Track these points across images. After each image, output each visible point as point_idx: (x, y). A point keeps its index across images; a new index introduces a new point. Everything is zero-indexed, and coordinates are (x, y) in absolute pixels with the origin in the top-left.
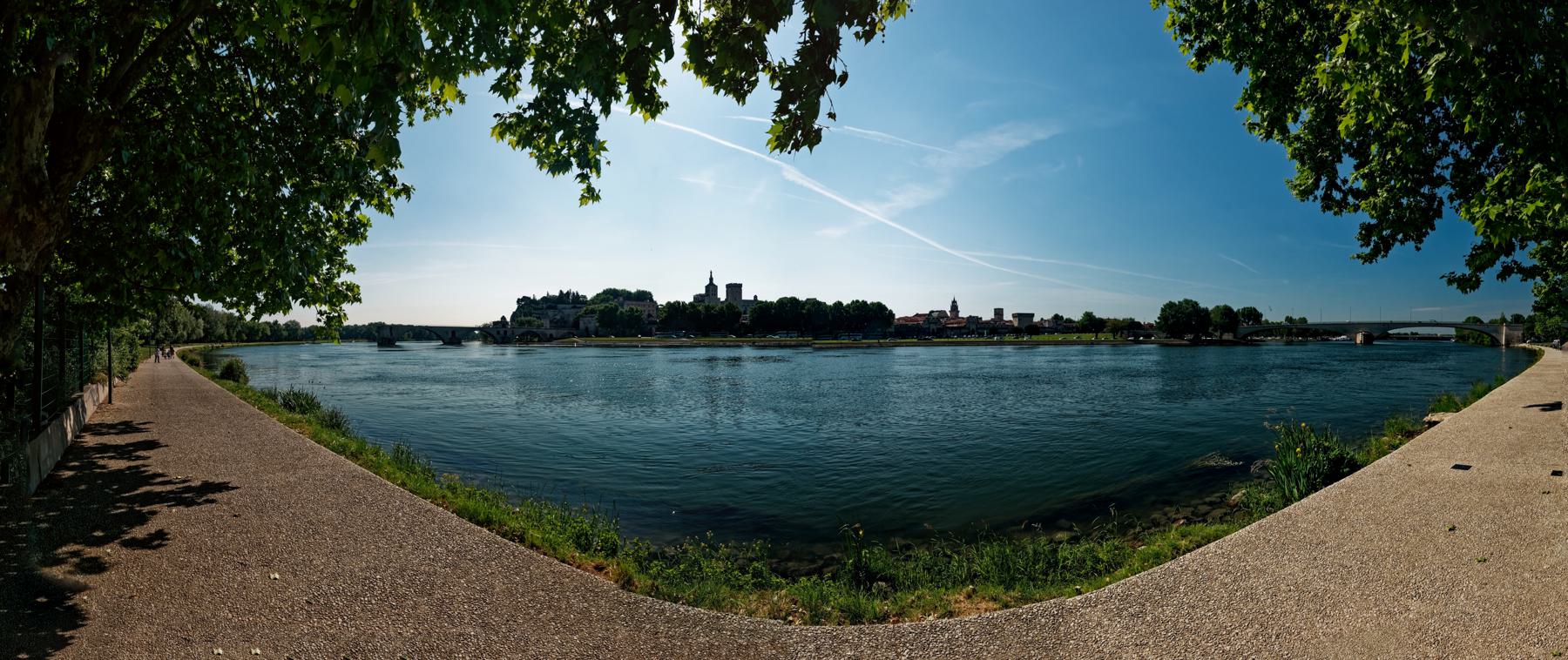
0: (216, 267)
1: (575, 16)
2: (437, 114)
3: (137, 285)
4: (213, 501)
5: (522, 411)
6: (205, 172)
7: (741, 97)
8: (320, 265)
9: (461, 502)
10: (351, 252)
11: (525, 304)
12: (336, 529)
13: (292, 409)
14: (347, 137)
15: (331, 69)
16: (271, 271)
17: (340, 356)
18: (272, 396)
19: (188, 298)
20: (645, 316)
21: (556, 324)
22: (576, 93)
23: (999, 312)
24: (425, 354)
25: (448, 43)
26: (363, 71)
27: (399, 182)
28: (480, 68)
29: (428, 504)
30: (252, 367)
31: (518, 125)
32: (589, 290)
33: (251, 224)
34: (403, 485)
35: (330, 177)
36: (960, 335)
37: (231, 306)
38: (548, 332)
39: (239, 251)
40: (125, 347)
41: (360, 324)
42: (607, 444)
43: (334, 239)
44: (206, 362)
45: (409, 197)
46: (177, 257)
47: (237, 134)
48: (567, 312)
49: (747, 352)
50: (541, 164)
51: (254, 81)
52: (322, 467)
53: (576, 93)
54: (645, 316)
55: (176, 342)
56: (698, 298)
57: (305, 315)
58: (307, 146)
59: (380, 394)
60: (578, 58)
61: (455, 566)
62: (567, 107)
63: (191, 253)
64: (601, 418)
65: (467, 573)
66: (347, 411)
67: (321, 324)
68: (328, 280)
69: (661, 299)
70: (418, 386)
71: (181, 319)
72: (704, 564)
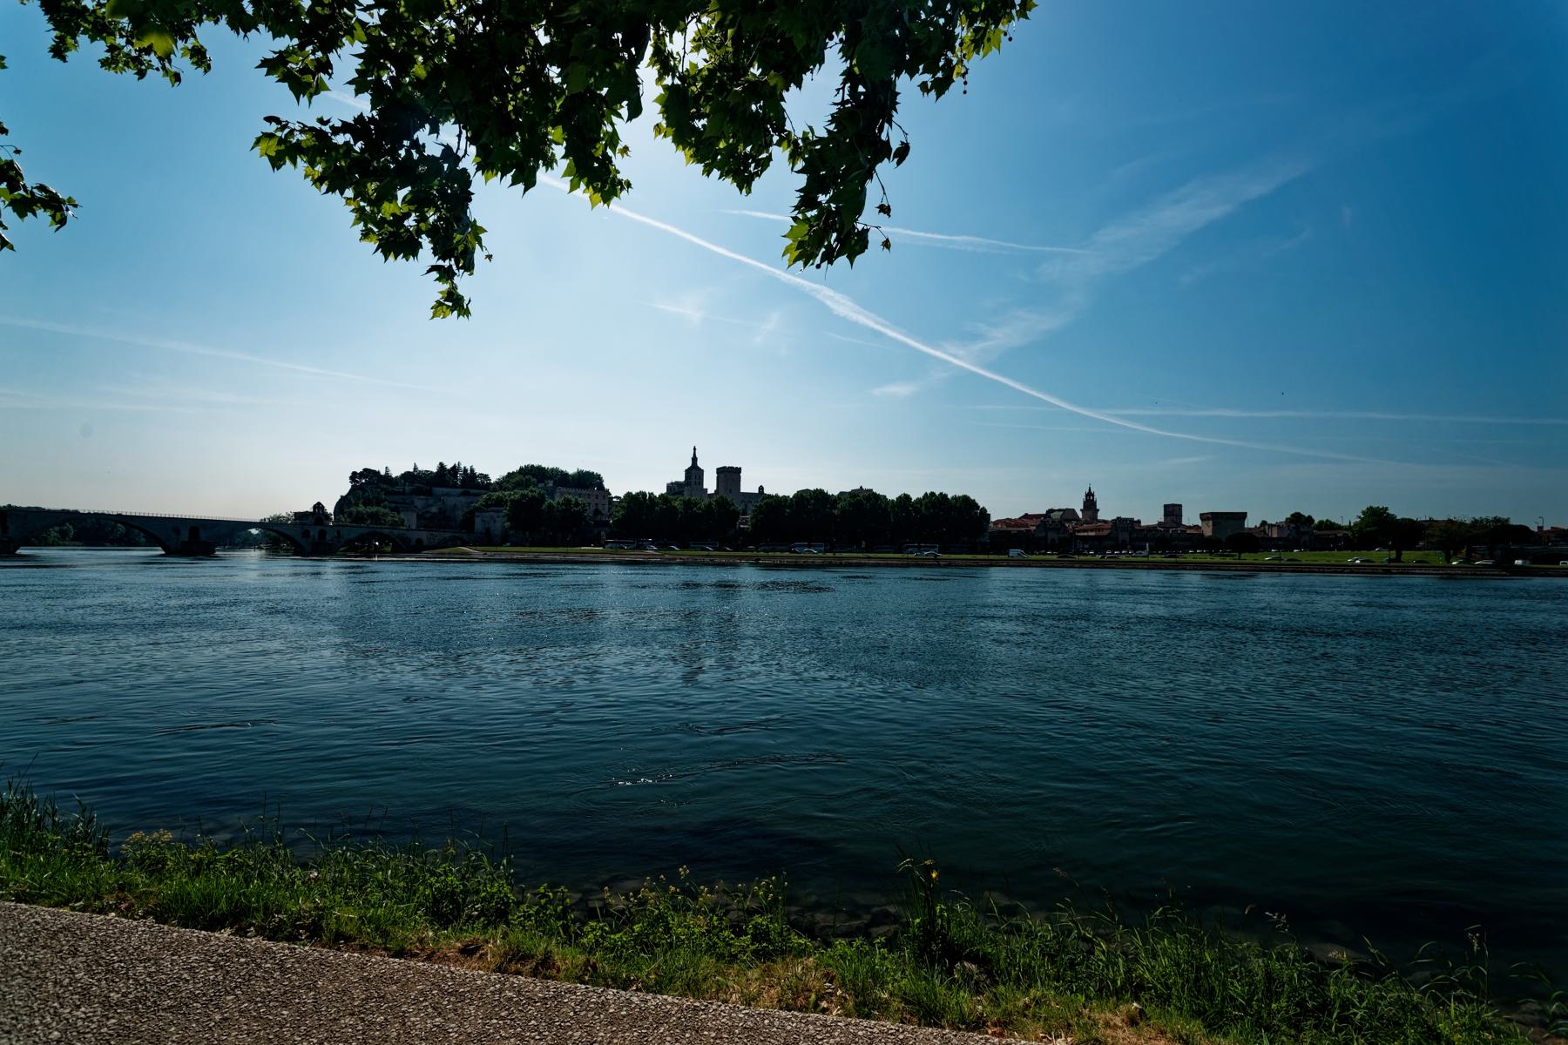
7: (745, 182)
11: (368, 484)
20: (589, 513)
21: (426, 521)
23: (1173, 511)
36: (1029, 550)
48: (451, 501)
54: (589, 513)
56: (673, 488)
69: (617, 487)
72: (673, 921)
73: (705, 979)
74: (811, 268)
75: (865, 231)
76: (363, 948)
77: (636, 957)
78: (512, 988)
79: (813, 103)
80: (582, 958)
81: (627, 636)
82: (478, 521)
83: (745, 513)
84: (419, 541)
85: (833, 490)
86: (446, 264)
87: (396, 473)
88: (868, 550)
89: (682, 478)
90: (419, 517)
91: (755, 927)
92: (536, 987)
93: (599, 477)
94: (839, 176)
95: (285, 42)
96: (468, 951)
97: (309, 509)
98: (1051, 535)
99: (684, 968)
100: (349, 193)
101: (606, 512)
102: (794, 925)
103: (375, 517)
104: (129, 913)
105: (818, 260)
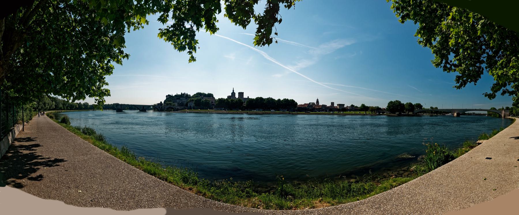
0: (59, 83)
3: (32, 90)
5: (167, 135)
6: (55, 50)
8: (96, 82)
9: (145, 167)
10: (107, 78)
11: (169, 97)
12: (101, 176)
13: (86, 134)
14: (106, 36)
15: (100, 11)
16: (78, 85)
17: (103, 115)
18: (79, 129)
19: (49, 94)
20: (210, 102)
22: (188, 22)
24: (133, 115)
25: (143, 3)
26: (112, 12)
27: (124, 53)
28: (154, 12)
29: (134, 168)
30: (72, 119)
31: (167, 33)
32: (192, 93)
33: (71, 68)
34: (125, 161)
35: (100, 51)
37: (64, 97)
38: (177, 107)
39: (67, 78)
40: (28, 112)
41: (110, 104)
42: (197, 147)
43: (101, 73)
44: (56, 117)
45: (128, 58)
46: (46, 80)
47: (67, 35)
48: (183, 100)
49: (245, 116)
50: (175, 47)
51: (73, 16)
52: (96, 154)
53: (188, 22)
54: (210, 102)
55: (45, 110)
56: (229, 97)
57: (90, 101)
58: (91, 40)
59: (117, 129)
60: (189, 10)
61: (143, 189)
62: (185, 27)
63: (51, 78)
64: (195, 138)
66: (105, 135)
67: (96, 104)
68: (99, 88)
69: (217, 97)
70: (131, 126)
71: (47, 102)
80: (210, 194)
87: (174, 95)
96: (190, 189)
103: (170, 104)
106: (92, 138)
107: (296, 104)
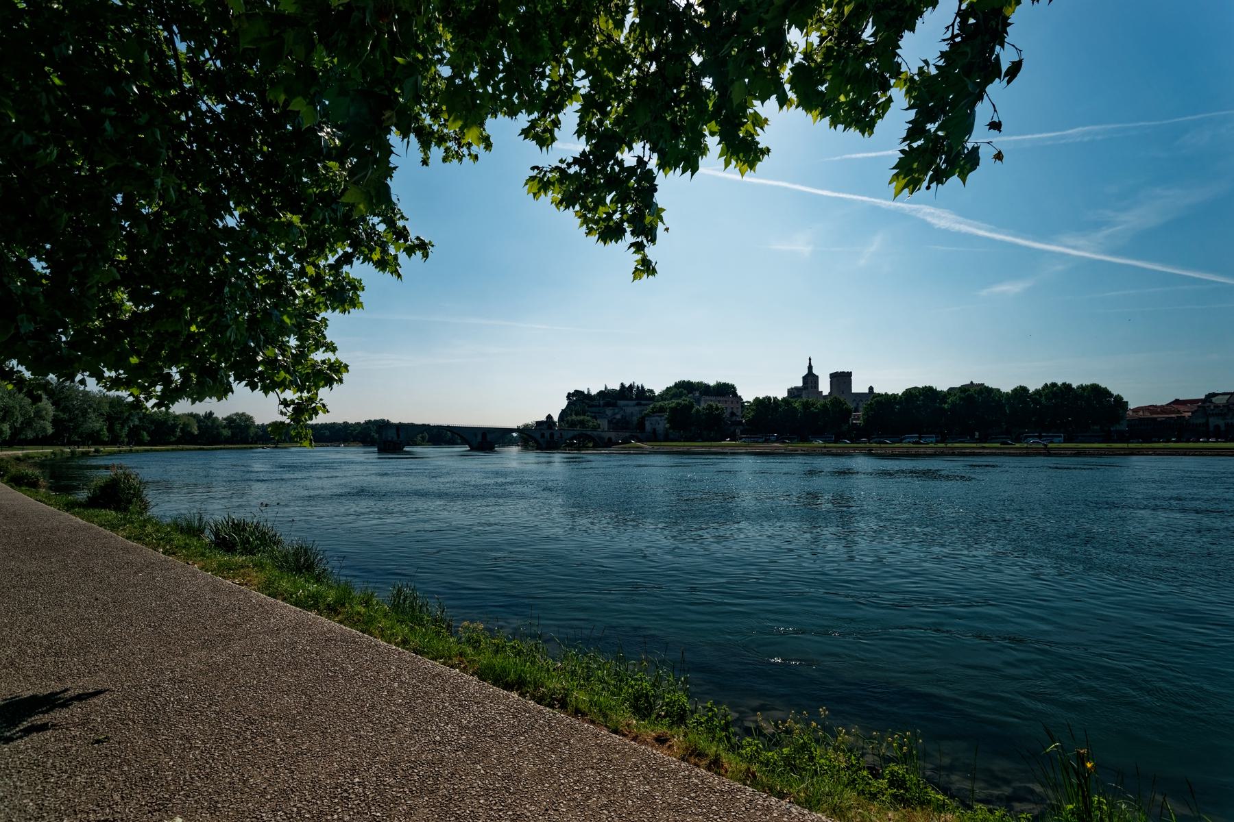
1: (629, 60)
2: (460, 158)
4: (43, 728)
9: (484, 659)
11: (577, 399)
17: (313, 466)
18: (192, 530)
20: (727, 414)
21: (616, 425)
25: (473, 76)
27: (412, 237)
28: (512, 112)
29: (438, 666)
32: (658, 384)
34: (404, 643)
37: (116, 383)
38: (607, 435)
41: (352, 421)
44: (61, 480)
45: (426, 256)
48: (629, 410)
49: (861, 463)
50: (590, 232)
54: (727, 414)
56: (793, 392)
57: (263, 407)
65: (486, 755)
69: (747, 394)
72: (818, 752)
73: (849, 808)
74: (922, 191)
75: (975, 150)
76: (593, 722)
77: (786, 774)
78: (697, 777)
79: (923, 45)
80: (744, 766)
81: (760, 512)
82: (647, 424)
83: (856, 410)
84: (610, 439)
85: (942, 386)
86: (639, 240)
87: (594, 392)
88: (980, 441)
89: (800, 384)
90: (609, 422)
91: (892, 773)
92: (713, 779)
93: (733, 387)
94: (948, 104)
95: (536, 115)
96: (661, 740)
97: (544, 419)
98: (1213, 421)
99: (829, 794)
100: (577, 208)
101: (739, 414)
102: (929, 781)
103: (582, 423)
104: (465, 670)
105: (925, 184)
106: (260, 566)
107: (1120, 403)
